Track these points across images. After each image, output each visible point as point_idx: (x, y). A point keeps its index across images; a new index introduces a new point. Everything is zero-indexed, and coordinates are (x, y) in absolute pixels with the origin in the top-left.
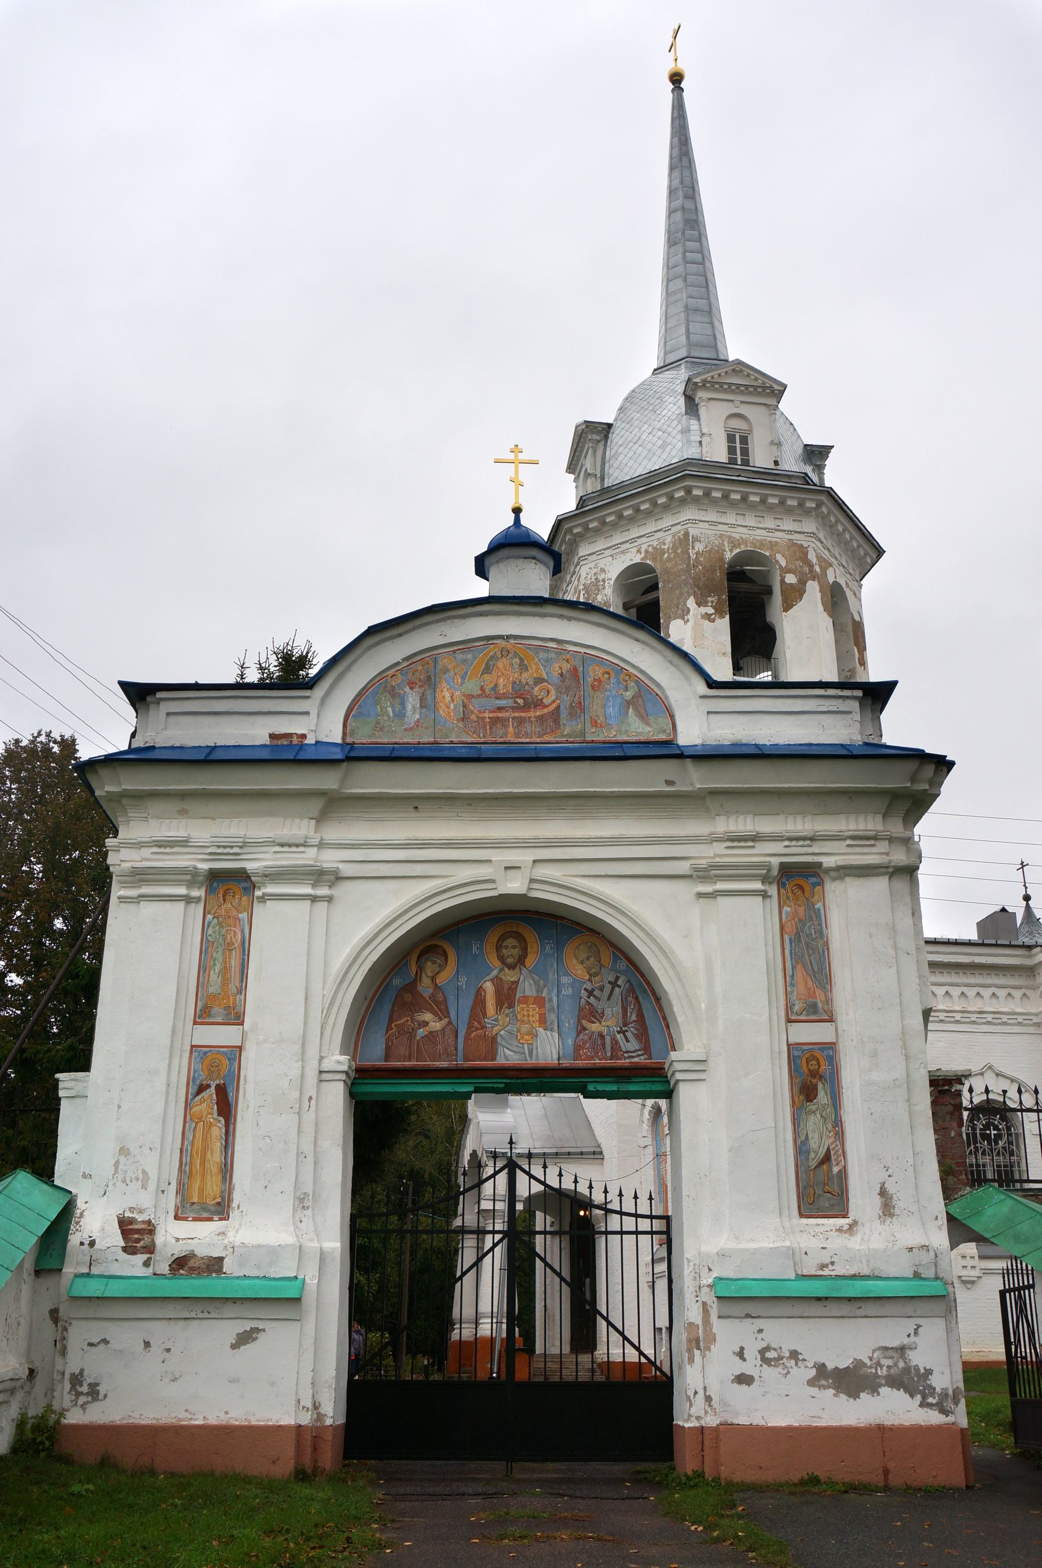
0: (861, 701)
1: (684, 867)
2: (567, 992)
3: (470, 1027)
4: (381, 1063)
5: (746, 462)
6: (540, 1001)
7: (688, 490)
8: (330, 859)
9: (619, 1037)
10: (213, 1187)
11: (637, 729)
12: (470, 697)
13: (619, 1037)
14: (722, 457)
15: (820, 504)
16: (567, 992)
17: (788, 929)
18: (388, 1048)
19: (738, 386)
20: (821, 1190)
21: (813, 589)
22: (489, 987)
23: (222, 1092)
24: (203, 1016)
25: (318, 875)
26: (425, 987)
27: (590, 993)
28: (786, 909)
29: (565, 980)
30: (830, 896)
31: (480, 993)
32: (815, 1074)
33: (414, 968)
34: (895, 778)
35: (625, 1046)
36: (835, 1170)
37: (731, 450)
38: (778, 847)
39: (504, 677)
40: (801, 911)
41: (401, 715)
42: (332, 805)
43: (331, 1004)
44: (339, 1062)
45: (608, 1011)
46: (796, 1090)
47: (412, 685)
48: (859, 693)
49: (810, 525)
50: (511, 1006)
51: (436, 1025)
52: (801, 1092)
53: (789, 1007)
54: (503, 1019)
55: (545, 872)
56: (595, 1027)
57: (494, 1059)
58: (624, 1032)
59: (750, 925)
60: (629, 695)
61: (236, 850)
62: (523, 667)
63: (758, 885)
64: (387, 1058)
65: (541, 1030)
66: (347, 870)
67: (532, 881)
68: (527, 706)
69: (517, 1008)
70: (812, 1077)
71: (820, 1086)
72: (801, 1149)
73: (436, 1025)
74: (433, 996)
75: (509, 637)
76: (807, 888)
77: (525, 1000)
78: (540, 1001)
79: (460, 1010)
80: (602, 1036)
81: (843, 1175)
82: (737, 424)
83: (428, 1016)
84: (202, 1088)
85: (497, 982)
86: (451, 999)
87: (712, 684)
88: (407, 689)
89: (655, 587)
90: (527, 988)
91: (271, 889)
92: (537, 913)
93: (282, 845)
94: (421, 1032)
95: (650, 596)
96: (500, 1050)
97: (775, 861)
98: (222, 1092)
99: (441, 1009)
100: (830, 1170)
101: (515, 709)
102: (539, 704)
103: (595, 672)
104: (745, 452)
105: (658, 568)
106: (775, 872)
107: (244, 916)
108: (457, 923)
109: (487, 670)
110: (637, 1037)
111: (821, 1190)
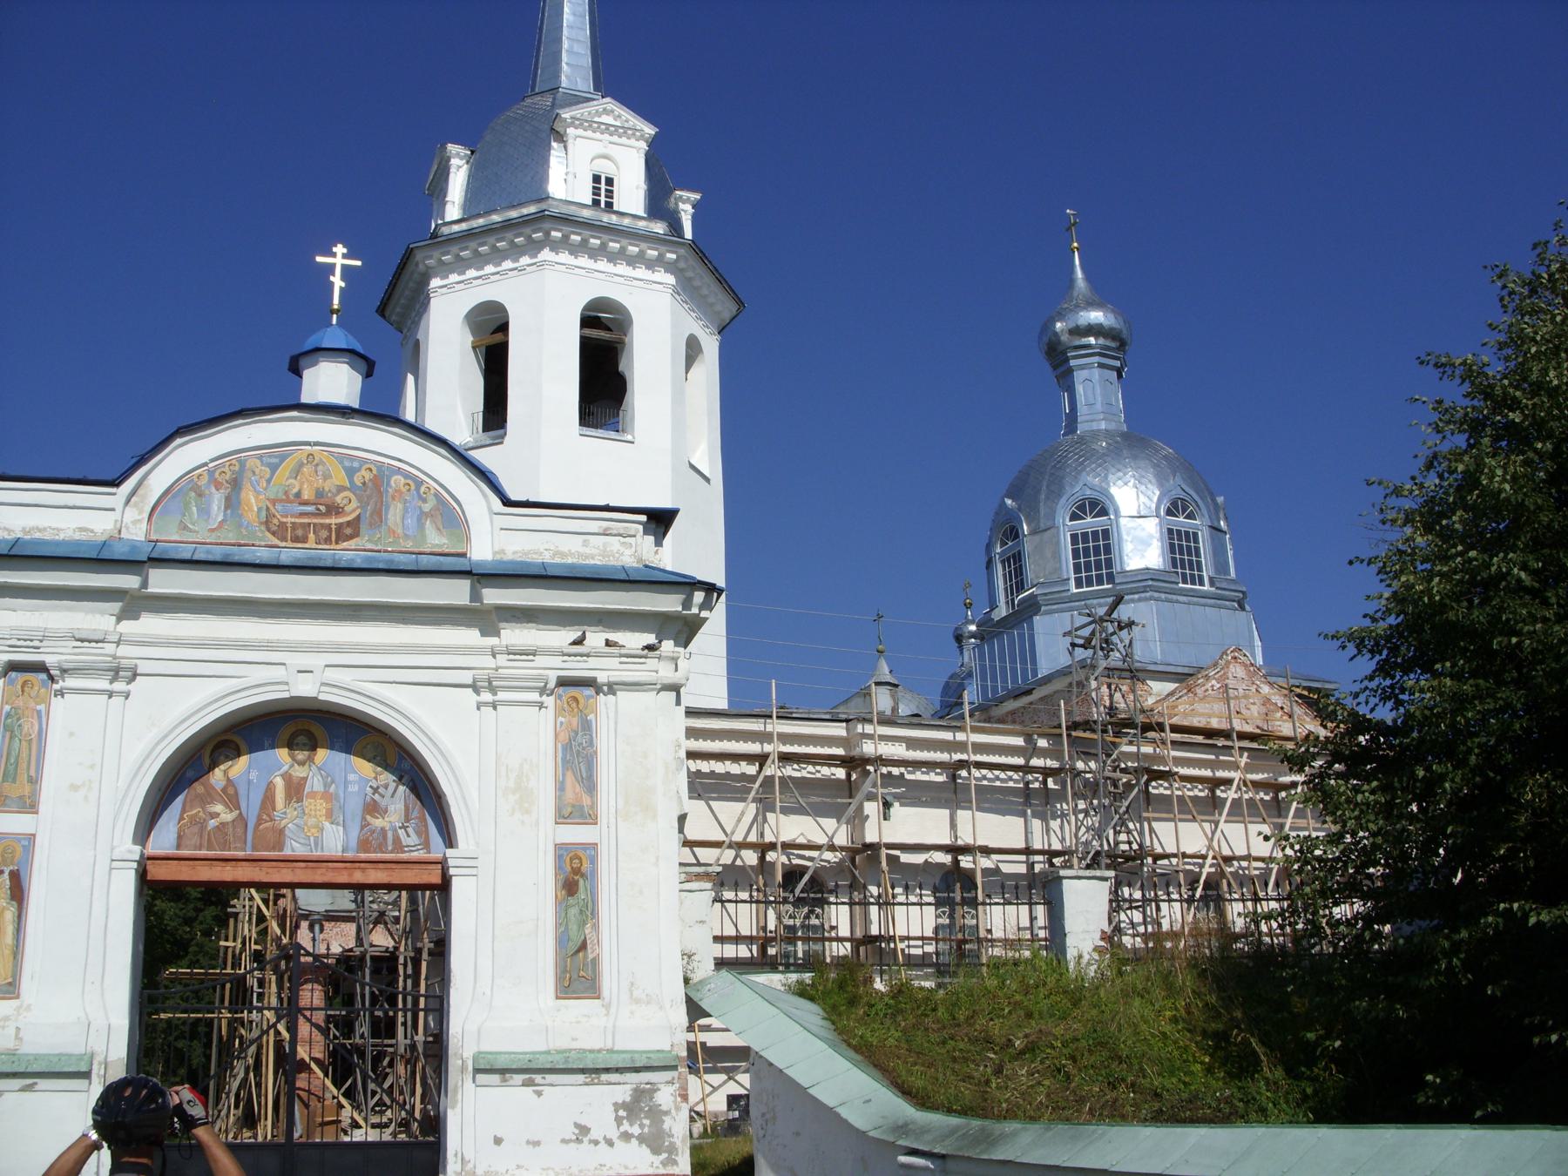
0: (645, 525)
1: (467, 677)
2: (353, 788)
3: (259, 821)
4: (172, 852)
5: (609, 205)
7: (547, 234)
9: (401, 832)
11: (435, 539)
12: (274, 502)
13: (401, 832)
14: (587, 199)
16: (353, 788)
17: (561, 737)
18: (180, 837)
20: (577, 973)
22: (279, 782)
27: (375, 790)
28: (561, 719)
29: (351, 777)
30: (601, 709)
31: (270, 789)
32: (577, 871)
33: (207, 761)
34: (669, 603)
35: (405, 840)
36: (591, 956)
37: (596, 191)
38: (557, 661)
40: (575, 721)
42: (134, 605)
43: (124, 797)
44: (130, 851)
45: (391, 808)
46: (560, 885)
47: (218, 486)
48: (643, 518)
50: (300, 800)
51: (228, 817)
52: (564, 886)
54: (291, 813)
55: (333, 675)
56: (378, 823)
57: (281, 849)
58: (403, 827)
60: (427, 507)
61: (36, 643)
63: (535, 696)
64: (178, 847)
65: (327, 824)
66: (143, 667)
67: (323, 684)
68: (328, 513)
69: (305, 803)
70: (575, 878)
71: (581, 882)
72: (561, 940)
73: (228, 817)
74: (224, 790)
75: (317, 444)
76: (582, 701)
77: (313, 795)
79: (251, 805)
80: (383, 829)
81: (595, 962)
82: (605, 169)
83: (218, 808)
85: (287, 778)
86: (242, 792)
87: (507, 502)
88: (213, 489)
89: (503, 328)
90: (315, 783)
91: (70, 682)
92: (328, 712)
93: (82, 641)
94: (213, 823)
95: (498, 337)
96: (288, 842)
97: (553, 677)
100: (585, 957)
101: (319, 514)
103: (397, 481)
104: (610, 194)
106: (552, 684)
107: (42, 707)
108: (251, 720)
110: (418, 833)
111: (577, 973)
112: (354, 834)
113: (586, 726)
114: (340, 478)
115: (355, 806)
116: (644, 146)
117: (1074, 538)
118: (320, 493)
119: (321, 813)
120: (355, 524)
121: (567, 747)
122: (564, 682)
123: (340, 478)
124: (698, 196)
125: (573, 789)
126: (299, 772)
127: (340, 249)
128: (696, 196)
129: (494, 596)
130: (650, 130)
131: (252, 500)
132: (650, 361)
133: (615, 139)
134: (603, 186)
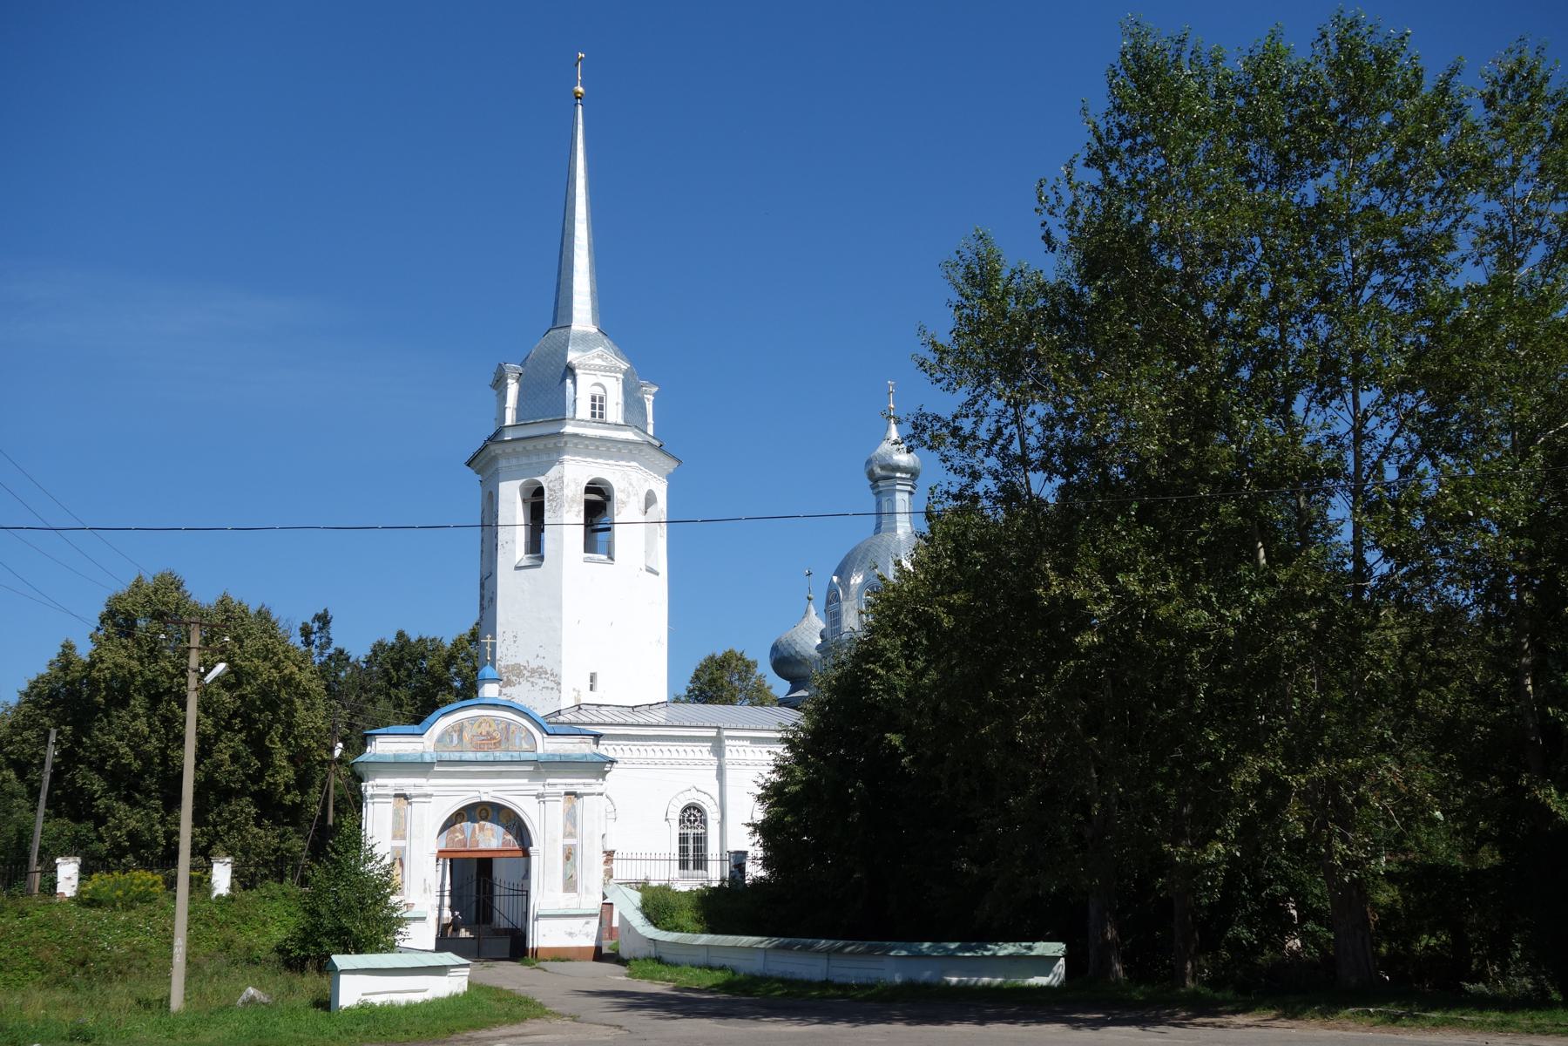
8: (428, 790)
20: (570, 884)
24: (394, 837)
25: (426, 796)
37: (593, 407)
39: (484, 729)
59: (557, 808)
72: (565, 874)
82: (598, 391)
104: (601, 408)
111: (570, 884)
114: (494, 726)
116: (621, 376)
119: (490, 838)
122: (567, 794)
123: (494, 726)
124: (655, 389)
125: (569, 827)
128: (655, 389)
130: (624, 366)
131: (467, 736)
132: (626, 509)
134: (598, 405)
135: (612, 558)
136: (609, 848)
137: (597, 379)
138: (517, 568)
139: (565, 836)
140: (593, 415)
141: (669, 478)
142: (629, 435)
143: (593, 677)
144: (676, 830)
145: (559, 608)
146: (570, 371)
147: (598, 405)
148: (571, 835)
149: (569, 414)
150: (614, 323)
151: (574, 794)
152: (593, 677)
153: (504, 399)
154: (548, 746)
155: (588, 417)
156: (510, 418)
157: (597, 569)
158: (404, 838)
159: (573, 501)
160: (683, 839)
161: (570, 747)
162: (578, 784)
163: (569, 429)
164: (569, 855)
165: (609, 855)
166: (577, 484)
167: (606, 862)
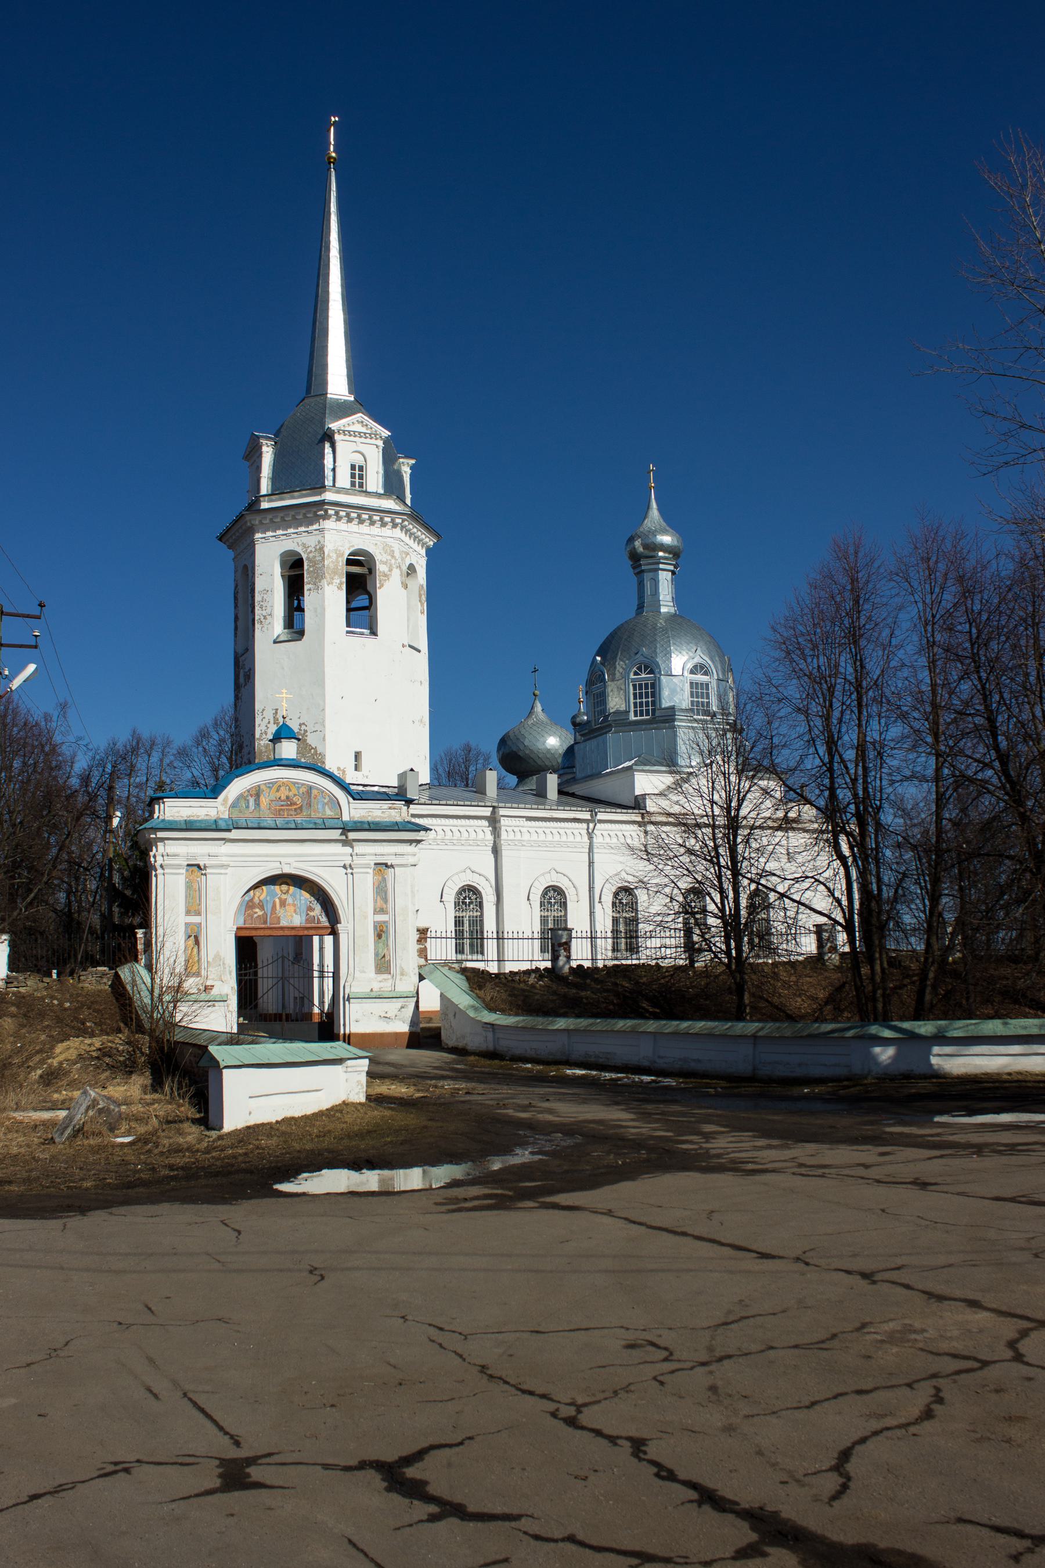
6: (294, 905)
10: (195, 968)
11: (329, 813)
15: (403, 520)
19: (360, 433)
21: (396, 572)
22: (277, 901)
23: (196, 937)
24: (188, 913)
25: (222, 866)
26: (256, 900)
37: (353, 476)
38: (374, 857)
39: (283, 793)
41: (248, 807)
49: (398, 532)
51: (260, 913)
53: (375, 910)
54: (282, 911)
56: (312, 914)
62: (290, 790)
66: (232, 864)
72: (376, 954)
78: (294, 905)
82: (358, 460)
83: (257, 910)
84: (190, 936)
85: (280, 899)
90: (290, 900)
98: (196, 937)
99: (262, 908)
102: (295, 804)
103: (314, 792)
104: (361, 477)
105: (304, 556)
109: (278, 790)
111: (383, 965)
112: (304, 918)
113: (384, 880)
114: (294, 791)
115: (304, 908)
116: (380, 443)
117: (634, 686)
118: (288, 797)
119: (294, 912)
120: (301, 808)
121: (378, 888)
124: (413, 462)
125: (380, 902)
126: (284, 897)
127: (284, 691)
128: (413, 462)
129: (352, 835)
130: (386, 433)
131: (264, 801)
133: (363, 440)
134: (358, 472)
135: (374, 633)
136: (422, 925)
137: (357, 447)
138: (275, 642)
139: (375, 912)
140: (353, 484)
141: (429, 552)
142: (390, 504)
143: (357, 756)
144: (451, 913)
145: (320, 683)
146: (329, 437)
147: (358, 472)
148: (382, 911)
149: (328, 482)
150: (368, 396)
151: (386, 865)
152: (357, 756)
153: (259, 469)
154: (354, 811)
155: (348, 486)
156: (265, 487)
157: (362, 642)
158: (198, 913)
159: (335, 573)
160: (459, 922)
161: (378, 813)
162: (387, 852)
163: (329, 496)
164: (381, 933)
165: (423, 934)
166: (340, 555)
167: (419, 941)
